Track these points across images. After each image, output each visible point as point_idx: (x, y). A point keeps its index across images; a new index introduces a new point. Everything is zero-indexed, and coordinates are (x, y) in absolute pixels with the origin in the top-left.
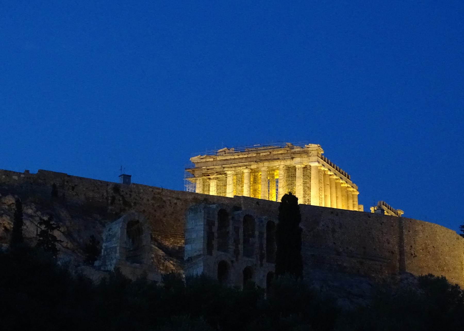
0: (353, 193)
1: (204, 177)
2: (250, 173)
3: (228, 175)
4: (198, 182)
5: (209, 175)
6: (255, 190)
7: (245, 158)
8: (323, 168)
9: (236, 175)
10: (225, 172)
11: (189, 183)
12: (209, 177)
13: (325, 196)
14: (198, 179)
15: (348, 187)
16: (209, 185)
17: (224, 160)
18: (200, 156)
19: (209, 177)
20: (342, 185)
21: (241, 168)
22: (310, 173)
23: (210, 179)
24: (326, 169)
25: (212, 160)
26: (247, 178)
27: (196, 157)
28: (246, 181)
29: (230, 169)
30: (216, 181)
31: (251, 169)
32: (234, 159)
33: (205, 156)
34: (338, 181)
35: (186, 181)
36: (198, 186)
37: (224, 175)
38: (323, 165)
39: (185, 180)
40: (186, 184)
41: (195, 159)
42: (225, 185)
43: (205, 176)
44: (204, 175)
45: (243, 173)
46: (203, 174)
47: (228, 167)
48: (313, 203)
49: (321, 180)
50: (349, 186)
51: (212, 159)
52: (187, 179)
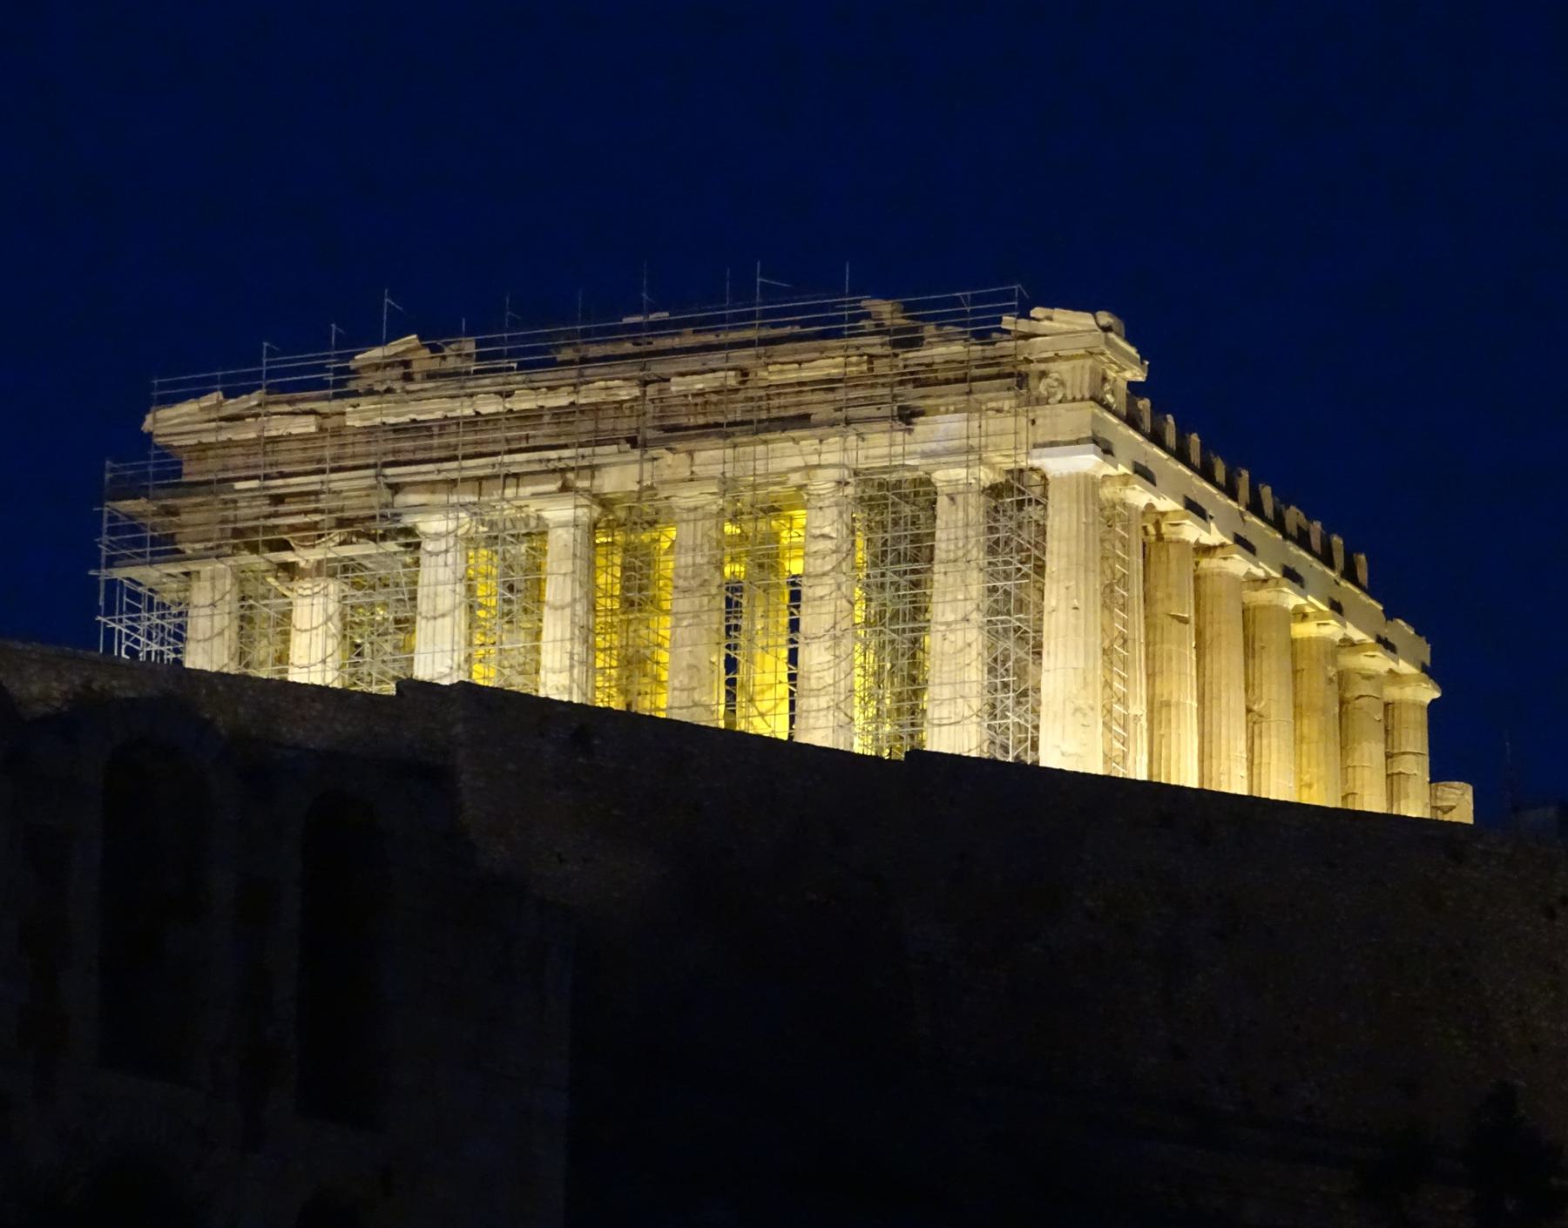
0: (1393, 693)
1: (247, 558)
2: (594, 526)
3: (429, 546)
4: (201, 594)
5: (285, 546)
6: (635, 662)
7: (557, 413)
8: (1139, 496)
9: (492, 540)
10: (407, 521)
11: (136, 599)
12: (288, 557)
13: (1157, 709)
14: (206, 568)
15: (1348, 643)
16: (287, 615)
17: (397, 429)
18: (214, 398)
19: (288, 557)
20: (1301, 630)
21: (526, 490)
22: (1042, 530)
23: (290, 569)
24: (1167, 504)
25: (307, 425)
26: (567, 566)
27: (189, 408)
28: (558, 588)
29: (441, 498)
30: (334, 587)
31: (605, 503)
32: (476, 422)
33: (253, 400)
34: (1263, 596)
35: (112, 584)
36: (199, 625)
37: (391, 546)
38: (1144, 473)
39: (104, 574)
40: (109, 611)
41: (177, 422)
42: (405, 625)
43: (253, 548)
44: (244, 539)
45: (538, 534)
46: (238, 533)
47: (431, 486)
48: (1050, 758)
49: (1124, 580)
50: (1357, 635)
51: (307, 425)
52: (120, 573)
